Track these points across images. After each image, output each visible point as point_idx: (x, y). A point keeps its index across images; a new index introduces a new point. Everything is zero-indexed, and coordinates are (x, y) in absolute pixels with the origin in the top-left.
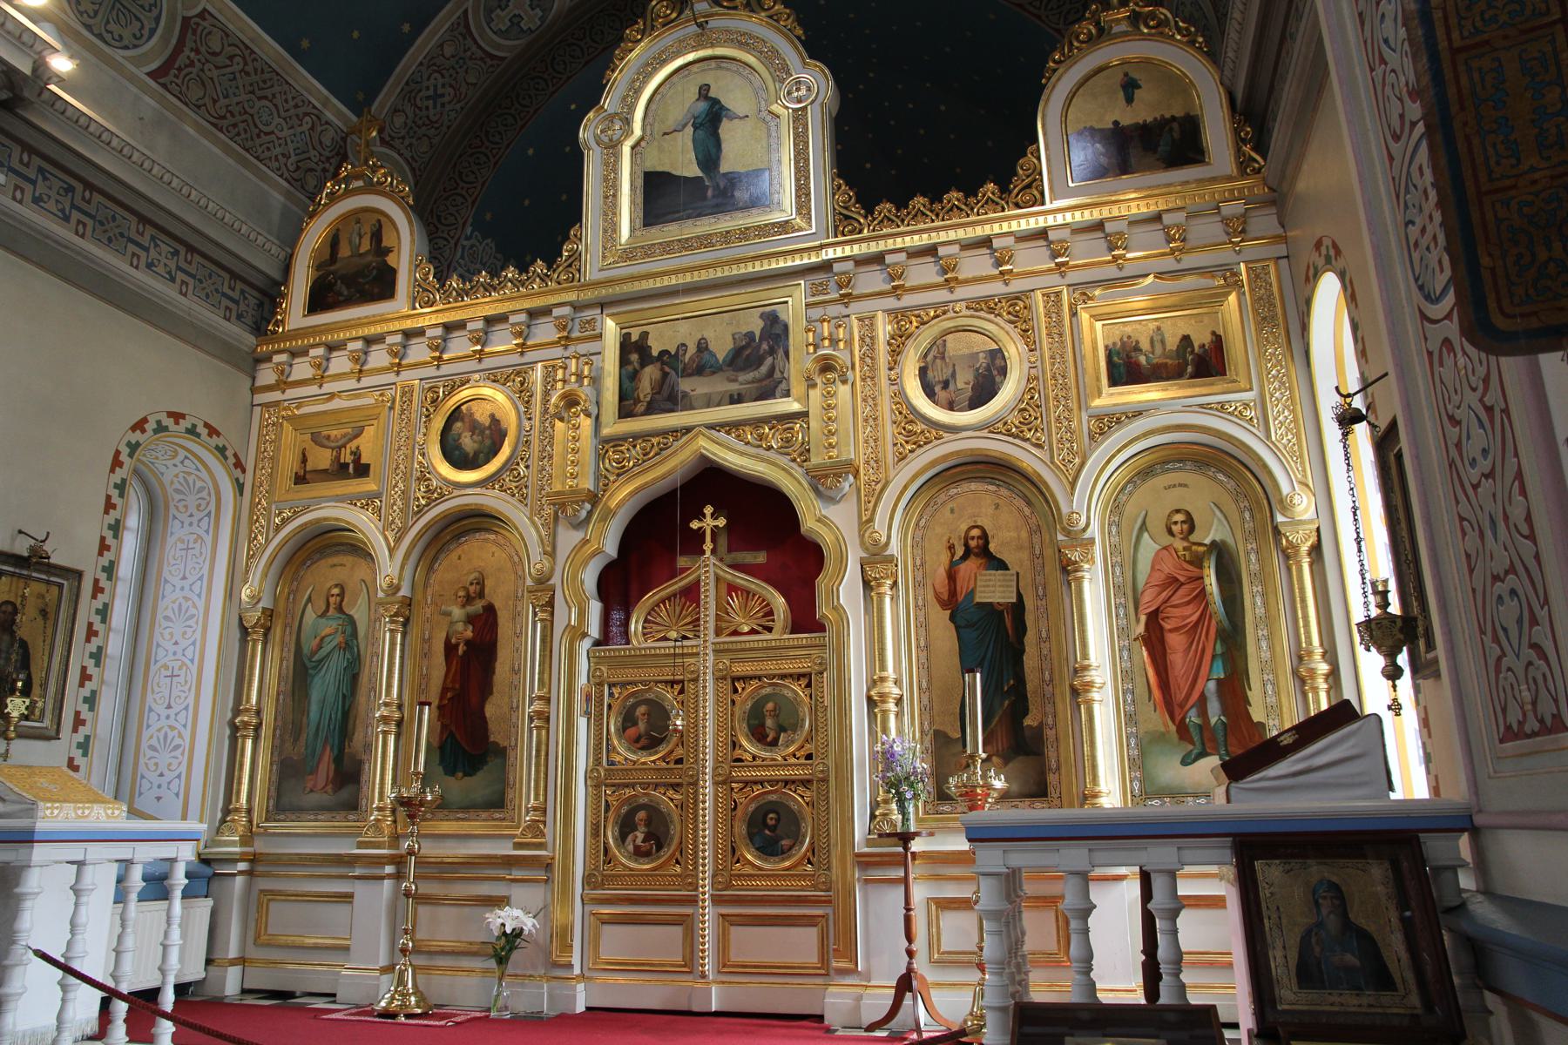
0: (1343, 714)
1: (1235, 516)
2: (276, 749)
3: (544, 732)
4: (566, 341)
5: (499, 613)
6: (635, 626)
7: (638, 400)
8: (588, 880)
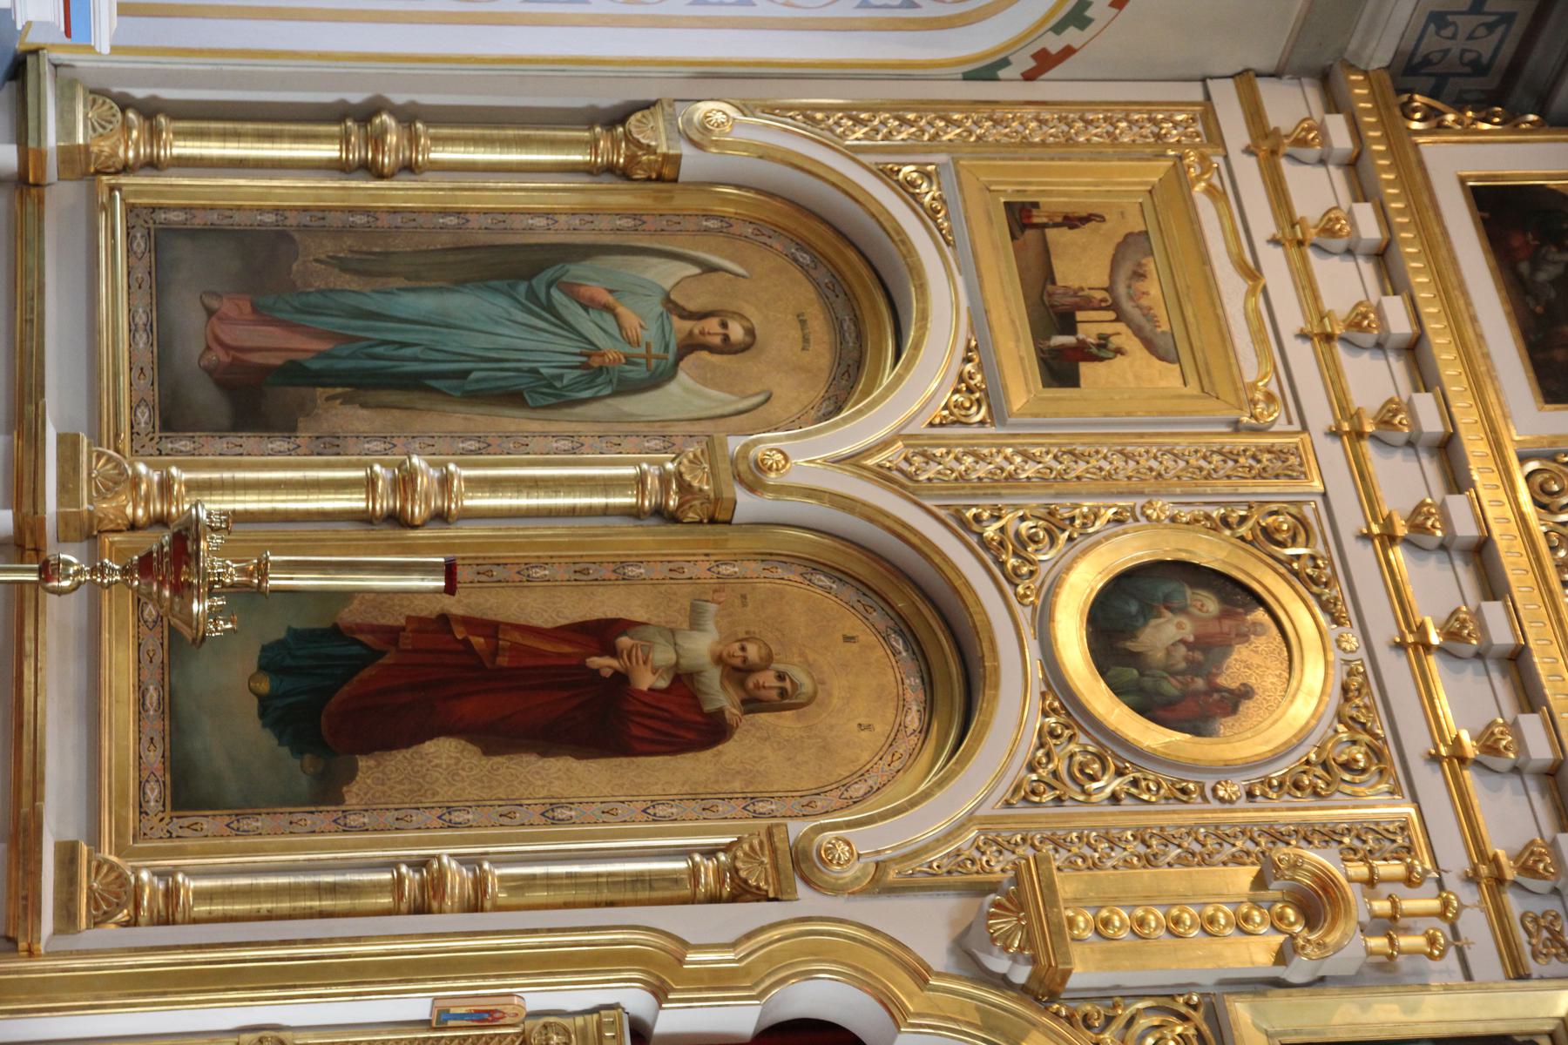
2: (317, 220)
3: (386, 901)
5: (707, 755)
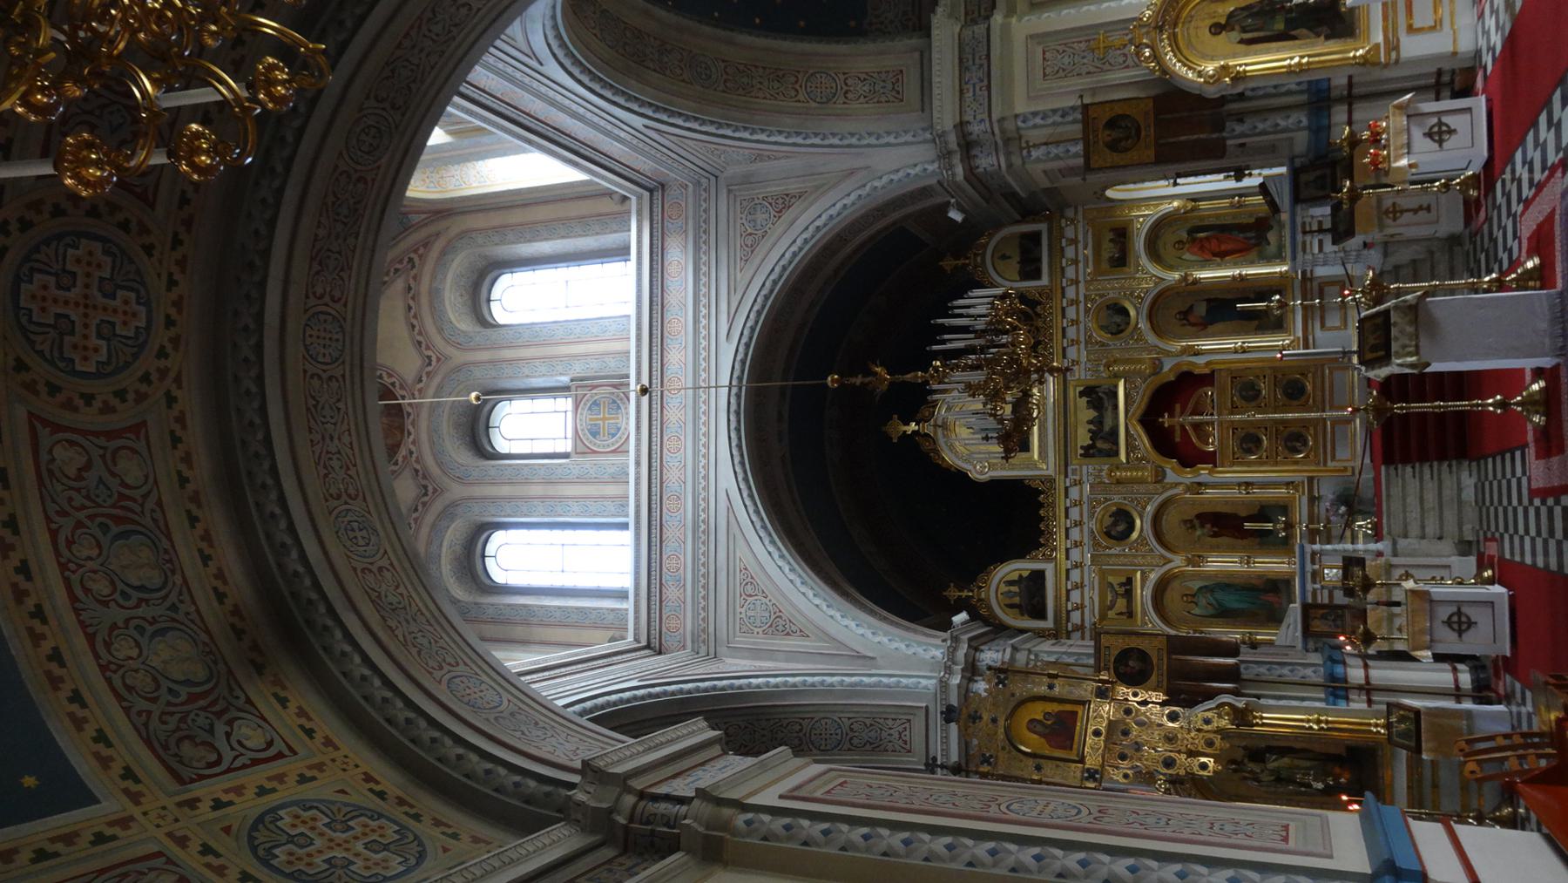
0: (1263, 186)
8: (1318, 464)
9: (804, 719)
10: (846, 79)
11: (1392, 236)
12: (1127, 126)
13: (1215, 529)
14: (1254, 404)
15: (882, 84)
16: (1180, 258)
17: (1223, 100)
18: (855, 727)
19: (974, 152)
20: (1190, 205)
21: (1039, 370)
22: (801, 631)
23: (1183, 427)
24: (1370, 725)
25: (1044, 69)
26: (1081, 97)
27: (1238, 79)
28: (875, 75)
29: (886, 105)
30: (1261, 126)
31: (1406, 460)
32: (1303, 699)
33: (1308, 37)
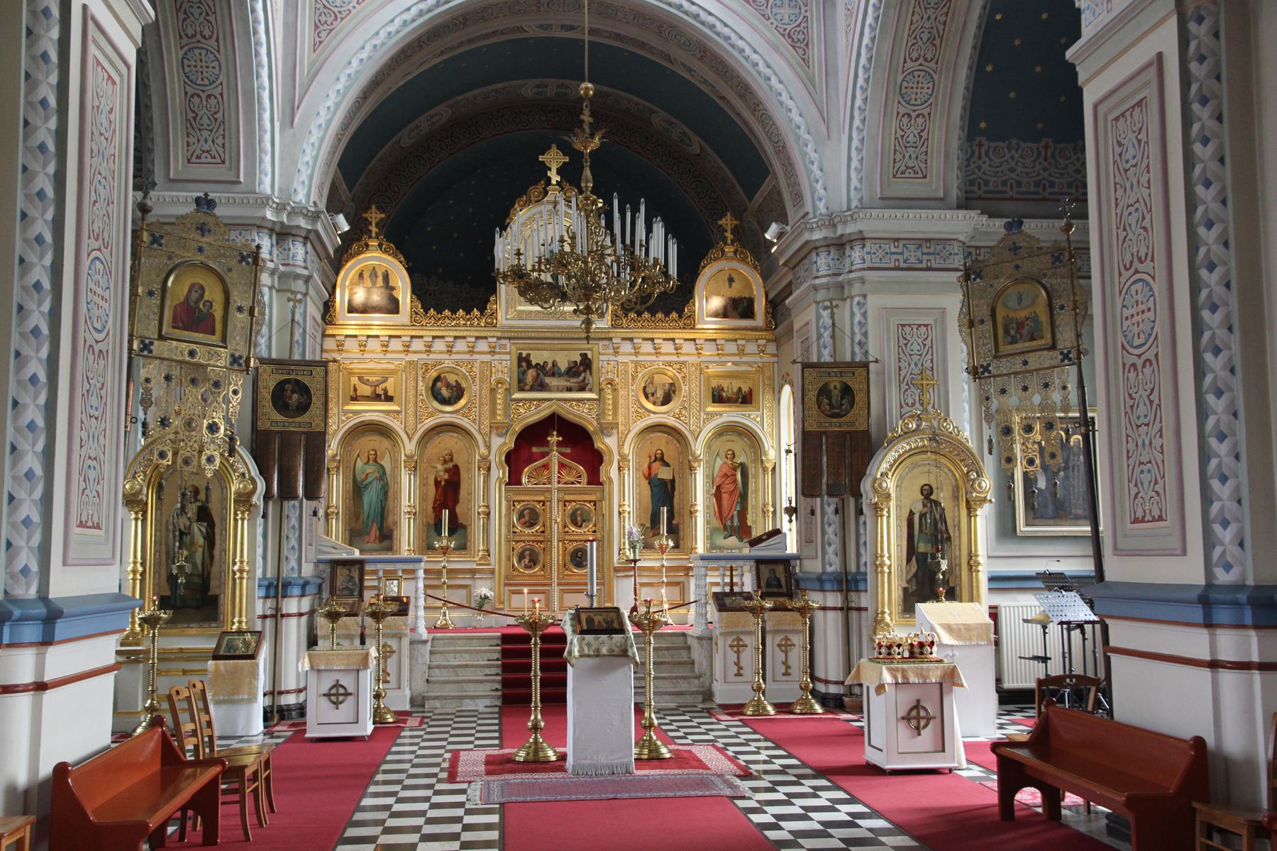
0: (777, 532)
1: (749, 454)
2: (346, 524)
4: (493, 353)
6: (524, 480)
7: (526, 384)
8: (507, 578)
9: (217, 40)
10: (924, 116)
11: (716, 644)
12: (842, 405)
13: (443, 483)
14: (568, 521)
15: (914, 156)
16: (718, 455)
17: (858, 495)
18: (212, 101)
19: (833, 250)
20: (770, 466)
21: (588, 309)
22: (321, 42)
23: (544, 455)
24: (240, 616)
25: (909, 325)
26: (877, 361)
27: (876, 508)
28: (924, 149)
29: (892, 161)
30: (830, 530)
31: (505, 653)
32: (264, 557)
33: (907, 573)
